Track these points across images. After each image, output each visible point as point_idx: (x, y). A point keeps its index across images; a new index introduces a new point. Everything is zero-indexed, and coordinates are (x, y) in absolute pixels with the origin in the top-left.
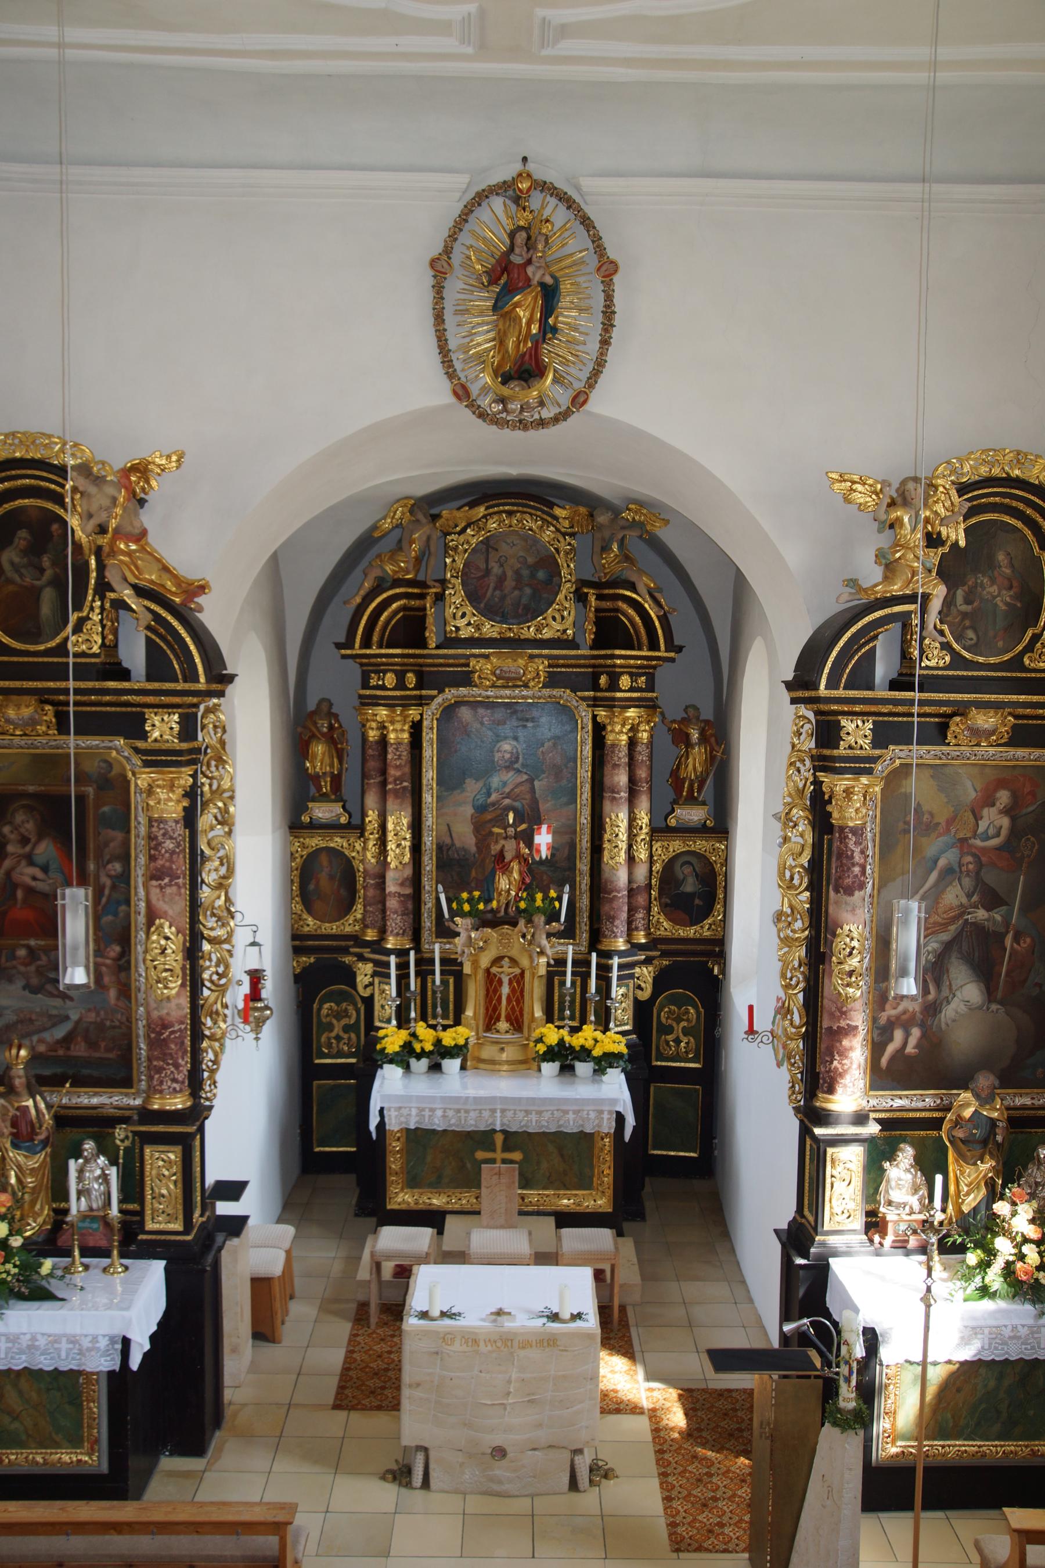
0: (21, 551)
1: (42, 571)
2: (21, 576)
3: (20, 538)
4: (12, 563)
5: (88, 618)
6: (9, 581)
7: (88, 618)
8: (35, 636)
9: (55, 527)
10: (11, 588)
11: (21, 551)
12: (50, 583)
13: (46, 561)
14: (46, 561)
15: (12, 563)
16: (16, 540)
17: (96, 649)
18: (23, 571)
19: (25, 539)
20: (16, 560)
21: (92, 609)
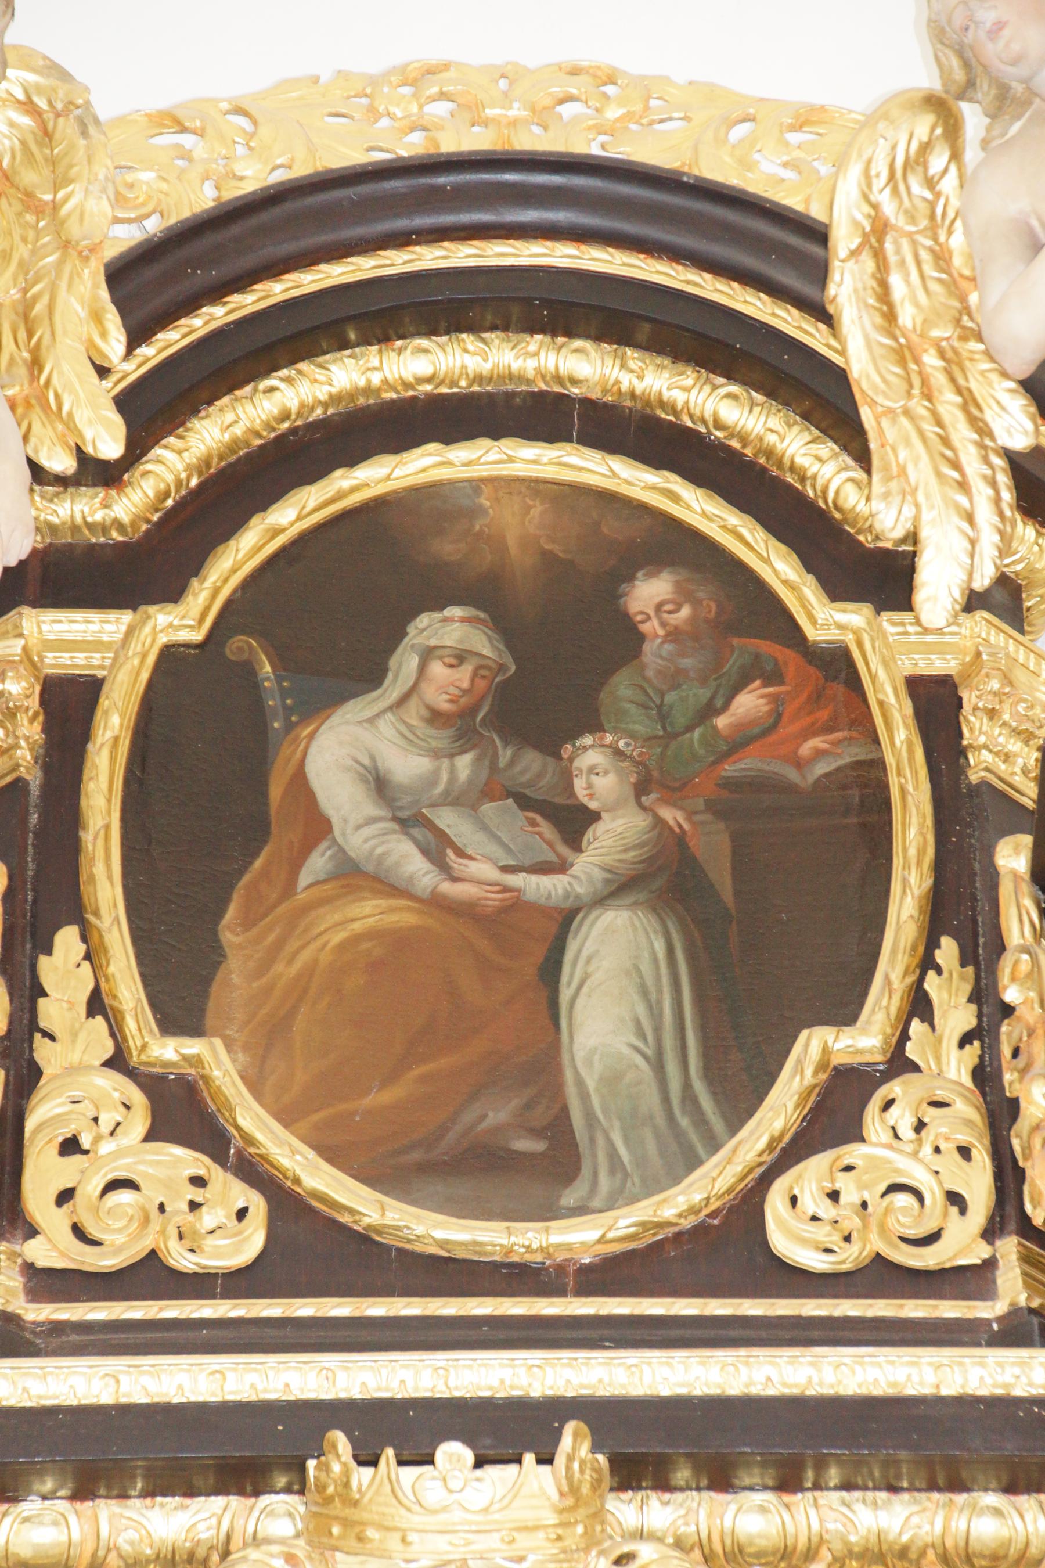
0: (435, 717)
1: (573, 822)
2: (439, 849)
3: (428, 654)
4: (380, 785)
5: (898, 1063)
6: (354, 877)
7: (898, 1063)
8: (546, 1165)
9: (650, 593)
10: (368, 913)
11: (435, 717)
12: (620, 887)
13: (596, 770)
14: (596, 770)
15: (380, 785)
16: (404, 664)
17: (961, 1244)
18: (448, 820)
19: (460, 657)
20: (407, 766)
21: (919, 1005)
